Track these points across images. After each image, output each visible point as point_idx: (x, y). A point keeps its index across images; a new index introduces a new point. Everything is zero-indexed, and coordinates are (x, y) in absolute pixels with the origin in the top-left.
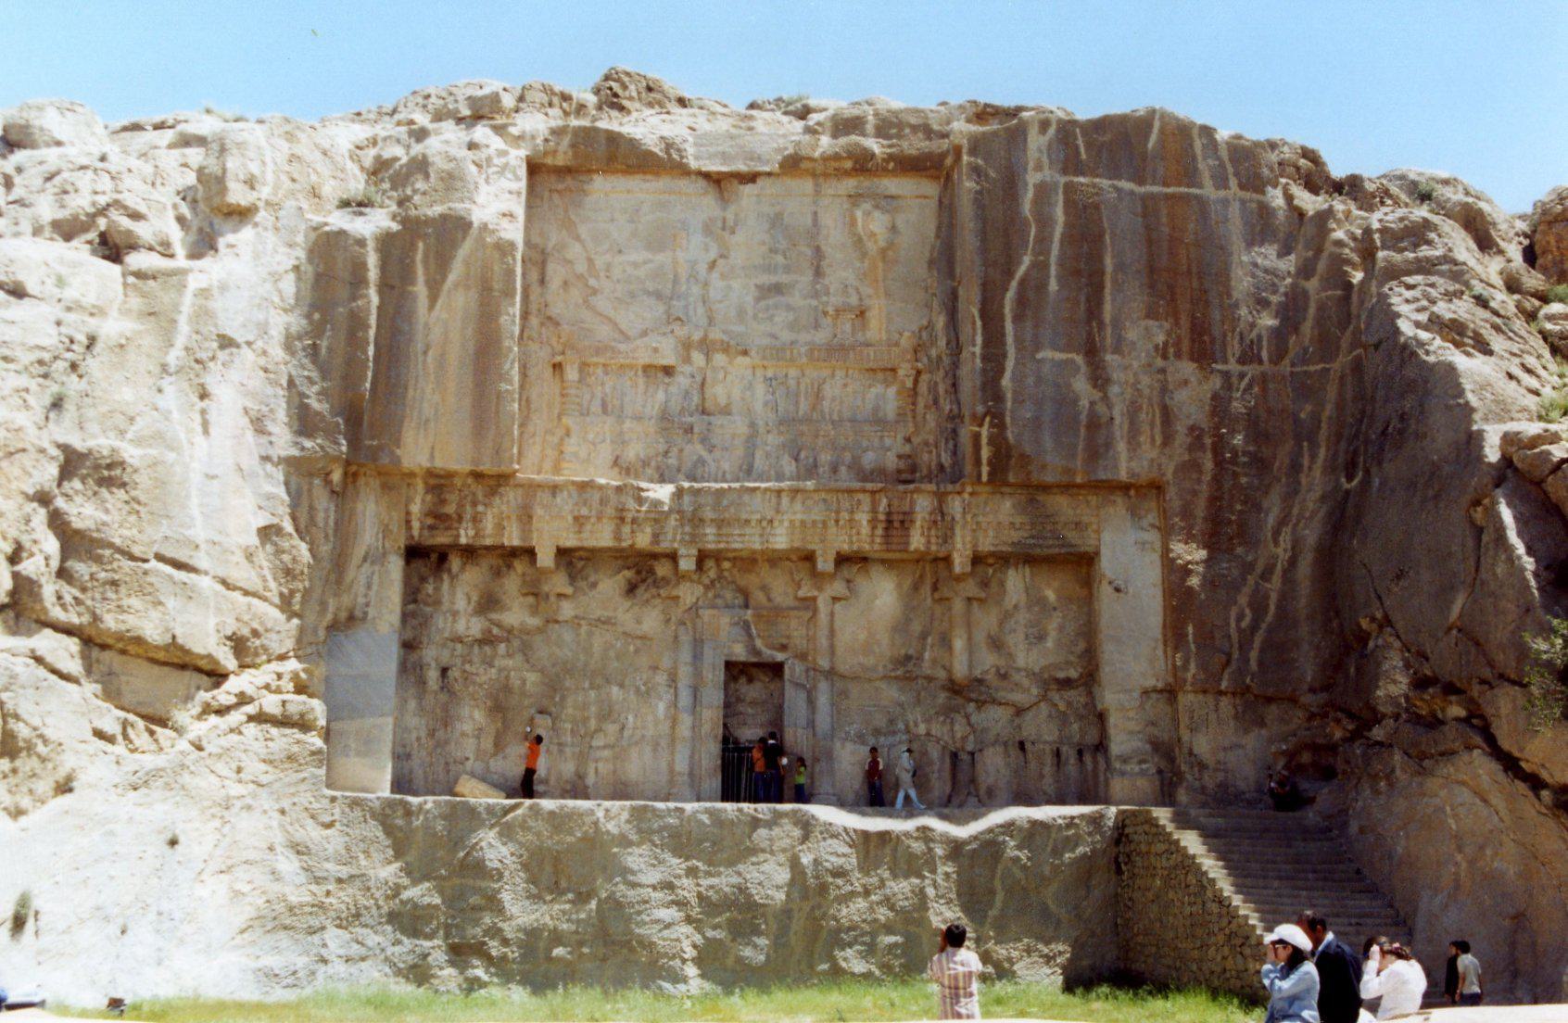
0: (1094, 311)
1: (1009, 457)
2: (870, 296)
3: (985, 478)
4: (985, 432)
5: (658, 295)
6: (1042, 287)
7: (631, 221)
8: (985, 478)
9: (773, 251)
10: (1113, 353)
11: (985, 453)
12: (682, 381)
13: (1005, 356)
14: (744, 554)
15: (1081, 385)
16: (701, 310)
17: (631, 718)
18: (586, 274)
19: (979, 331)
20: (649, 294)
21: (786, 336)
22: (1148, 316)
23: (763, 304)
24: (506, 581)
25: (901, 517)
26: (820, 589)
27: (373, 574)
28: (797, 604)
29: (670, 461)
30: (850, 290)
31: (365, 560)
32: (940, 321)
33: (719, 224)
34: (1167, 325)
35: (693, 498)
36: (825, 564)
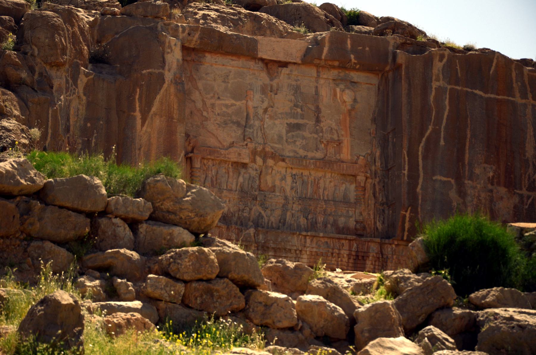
0: (460, 158)
2: (342, 135)
5: (238, 124)
8: (405, 238)
9: (296, 106)
10: (468, 180)
11: (407, 225)
13: (418, 177)
15: (453, 194)
16: (260, 134)
18: (202, 109)
19: (407, 163)
20: (234, 123)
21: (302, 153)
22: (486, 162)
23: (290, 134)
29: (245, 214)
30: (334, 131)
34: (494, 168)
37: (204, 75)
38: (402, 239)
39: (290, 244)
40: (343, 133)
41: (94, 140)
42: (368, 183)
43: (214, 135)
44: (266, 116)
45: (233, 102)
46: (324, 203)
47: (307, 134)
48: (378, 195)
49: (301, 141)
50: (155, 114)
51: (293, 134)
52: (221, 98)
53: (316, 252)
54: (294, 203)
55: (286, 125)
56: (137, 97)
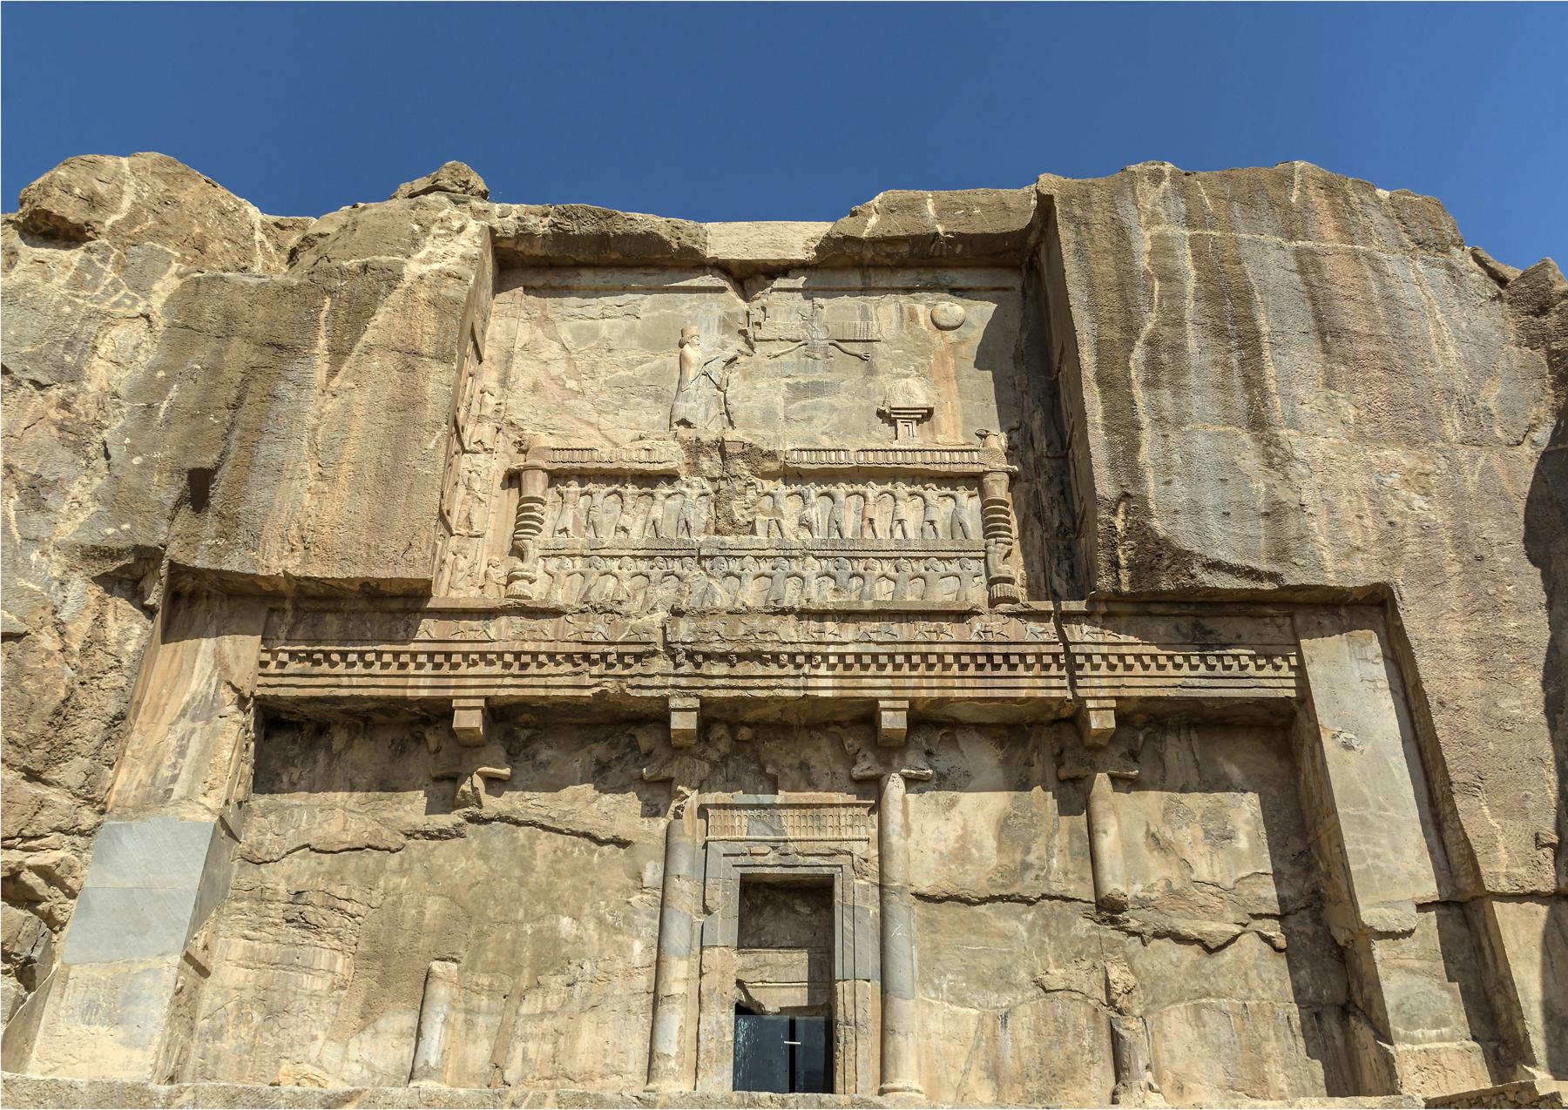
5: (658, 398)
6: (1178, 349)
14: (772, 713)
15: (1250, 460)
17: (587, 966)
18: (564, 377)
21: (826, 443)
25: (1003, 649)
26: (888, 766)
27: (193, 731)
31: (183, 714)
32: (1037, 421)
36: (893, 720)
39: (775, 638)
41: (165, 404)
48: (1048, 513)
50: (369, 350)
51: (803, 402)
53: (858, 656)
54: (805, 555)
55: (785, 388)
56: (323, 315)
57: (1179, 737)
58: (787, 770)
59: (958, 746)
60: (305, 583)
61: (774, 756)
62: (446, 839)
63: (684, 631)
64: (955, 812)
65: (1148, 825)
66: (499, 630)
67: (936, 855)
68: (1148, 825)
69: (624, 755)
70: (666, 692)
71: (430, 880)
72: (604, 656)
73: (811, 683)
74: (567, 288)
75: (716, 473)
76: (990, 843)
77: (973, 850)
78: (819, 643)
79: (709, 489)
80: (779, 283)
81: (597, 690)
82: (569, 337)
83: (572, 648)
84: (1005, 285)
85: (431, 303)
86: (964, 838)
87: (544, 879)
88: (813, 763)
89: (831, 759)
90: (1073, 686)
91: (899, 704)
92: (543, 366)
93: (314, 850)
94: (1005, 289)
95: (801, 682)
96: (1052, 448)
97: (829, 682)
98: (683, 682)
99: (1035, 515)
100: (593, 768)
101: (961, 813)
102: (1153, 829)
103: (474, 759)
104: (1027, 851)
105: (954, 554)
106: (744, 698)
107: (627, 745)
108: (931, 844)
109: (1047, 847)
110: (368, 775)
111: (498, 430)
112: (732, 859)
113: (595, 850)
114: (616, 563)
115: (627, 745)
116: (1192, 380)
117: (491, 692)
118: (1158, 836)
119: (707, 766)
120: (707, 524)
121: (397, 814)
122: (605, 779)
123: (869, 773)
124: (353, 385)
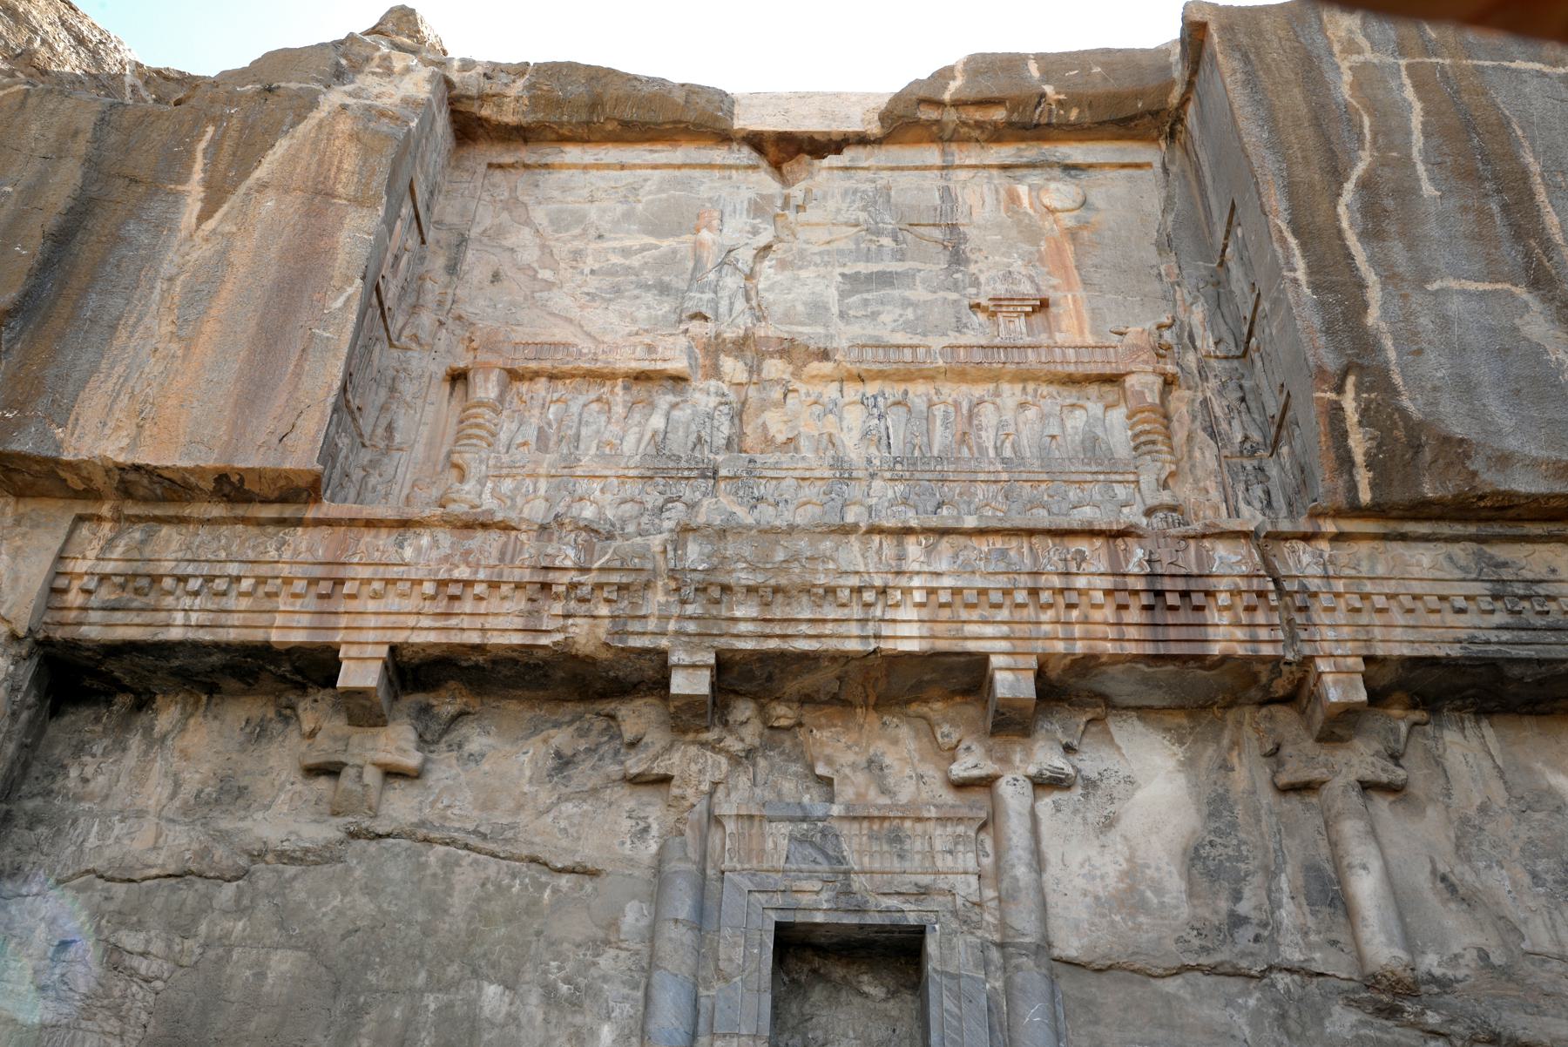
1: (1417, 448)
2: (1054, 287)
3: (1365, 496)
4: (1349, 403)
5: (663, 289)
6: (1407, 192)
7: (625, 200)
8: (1365, 496)
11: (1358, 443)
12: (703, 396)
18: (535, 265)
19: (1297, 252)
23: (856, 298)
24: (274, 748)
25: (1181, 585)
28: (949, 797)
33: (779, 203)
35: (708, 549)
37: (556, 194)
38: (1356, 511)
39: (831, 566)
40: (1055, 281)
42: (1180, 399)
43: (571, 321)
44: (766, 263)
45: (652, 240)
46: (1000, 467)
47: (919, 293)
48: (1224, 426)
49: (898, 311)
50: (263, 186)
51: (866, 296)
52: (607, 235)
53: (956, 591)
54: (873, 476)
55: (840, 279)
56: (203, 145)
57: (1463, 729)
58: (847, 771)
59: (1112, 740)
60: (132, 476)
61: (828, 751)
62: (317, 864)
63: (694, 553)
64: (1114, 836)
65: (1432, 861)
66: (419, 550)
67: (1089, 900)
68: (1432, 861)
69: (598, 745)
70: (664, 643)
71: (281, 925)
72: (573, 586)
73: (886, 630)
74: (546, 166)
75: (742, 377)
76: (1175, 884)
77: (1149, 894)
78: (898, 573)
79: (732, 397)
80: (832, 160)
81: (559, 637)
82: (545, 222)
83: (527, 576)
84: (1138, 161)
85: (354, 137)
86: (1133, 872)
87: (463, 925)
88: (887, 761)
89: (917, 757)
90: (1293, 638)
91: (1022, 662)
92: (507, 254)
93: (101, 877)
94: (1138, 166)
95: (870, 629)
96: (1222, 346)
97: (913, 630)
98: (691, 627)
99: (1204, 429)
100: (550, 763)
101: (1125, 838)
102: (1442, 868)
103: (369, 745)
104: (1237, 897)
105: (1089, 477)
106: (782, 655)
107: (601, 734)
108: (1080, 882)
109: (1269, 891)
110: (205, 768)
111: (441, 324)
112: (762, 897)
113: (544, 886)
114: (596, 485)
115: (601, 734)
116: (1432, 229)
117: (399, 637)
118: (1453, 878)
119: (723, 760)
120: (729, 440)
121: (241, 825)
122: (569, 778)
123: (976, 773)
124: (234, 229)
